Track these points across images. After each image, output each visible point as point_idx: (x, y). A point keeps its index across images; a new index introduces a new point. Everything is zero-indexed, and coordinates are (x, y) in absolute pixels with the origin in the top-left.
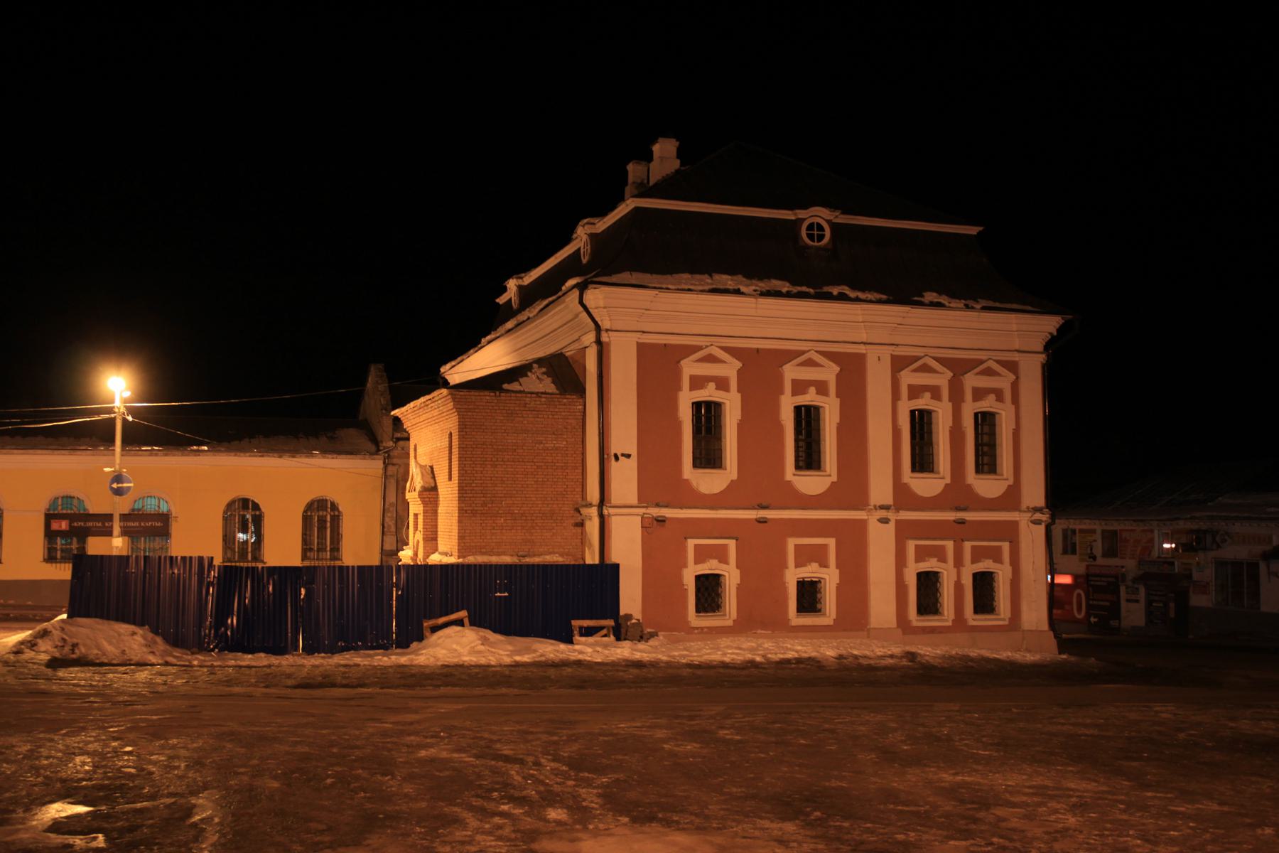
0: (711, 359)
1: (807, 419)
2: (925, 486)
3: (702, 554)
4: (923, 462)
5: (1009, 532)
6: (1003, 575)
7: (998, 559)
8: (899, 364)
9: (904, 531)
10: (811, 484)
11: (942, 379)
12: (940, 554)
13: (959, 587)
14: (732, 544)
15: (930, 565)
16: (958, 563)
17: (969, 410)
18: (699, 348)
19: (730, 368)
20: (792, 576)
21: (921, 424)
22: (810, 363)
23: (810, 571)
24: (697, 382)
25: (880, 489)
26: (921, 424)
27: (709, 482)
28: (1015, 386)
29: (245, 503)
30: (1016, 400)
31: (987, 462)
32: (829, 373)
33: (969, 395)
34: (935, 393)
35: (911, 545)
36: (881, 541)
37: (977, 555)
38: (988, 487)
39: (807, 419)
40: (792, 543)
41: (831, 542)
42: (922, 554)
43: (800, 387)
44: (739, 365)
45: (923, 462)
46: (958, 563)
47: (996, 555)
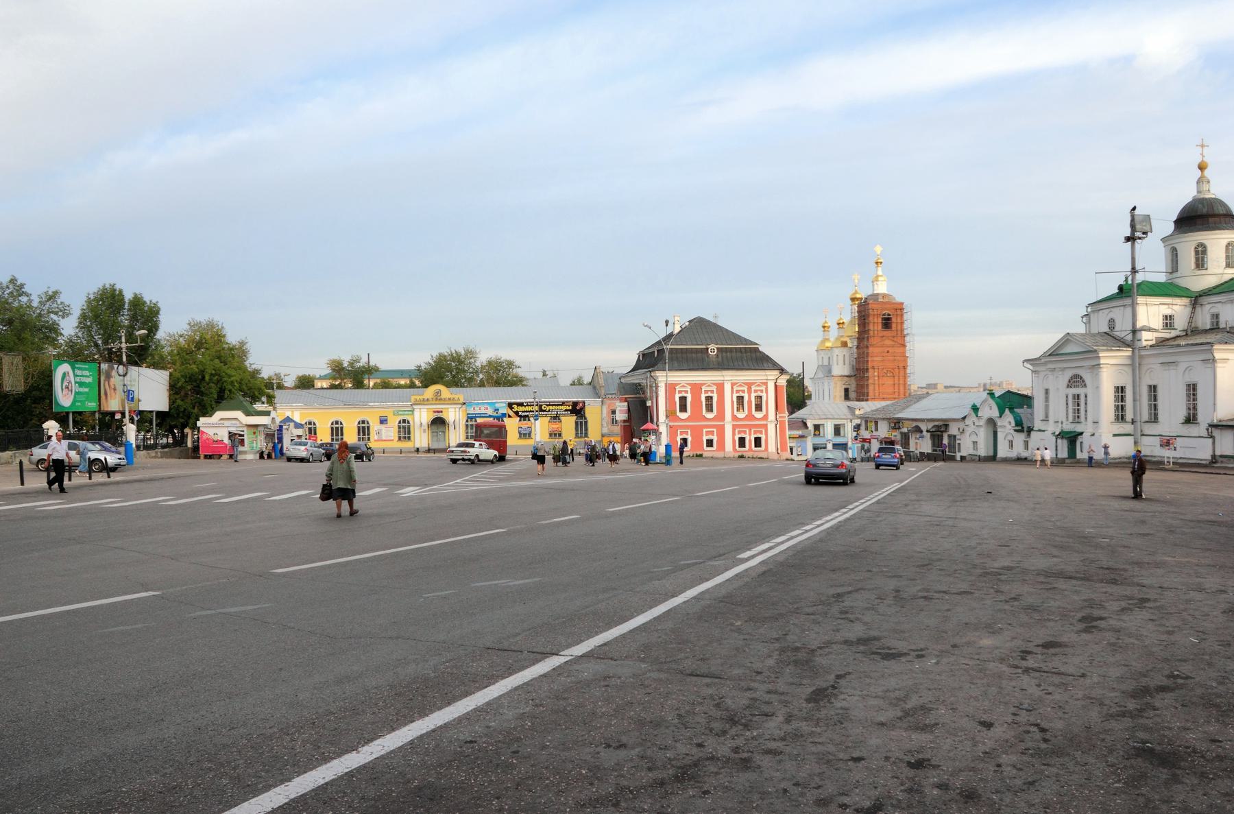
0: (683, 386)
1: (709, 399)
2: (741, 415)
3: (682, 433)
5: (765, 426)
7: (762, 433)
8: (733, 385)
9: (734, 427)
10: (710, 416)
11: (745, 388)
12: (745, 432)
13: (750, 441)
14: (689, 431)
16: (750, 434)
17: (753, 395)
18: (679, 384)
19: (688, 389)
20: (705, 438)
21: (740, 399)
22: (709, 386)
23: (710, 437)
24: (680, 392)
26: (740, 399)
27: (683, 416)
28: (766, 389)
30: (767, 393)
31: (759, 408)
32: (714, 388)
33: (703, 392)
34: (743, 391)
35: (737, 431)
38: (759, 415)
39: (709, 399)
40: (704, 430)
41: (715, 430)
42: (739, 432)
43: (706, 392)
44: (690, 387)
46: (750, 434)
47: (761, 433)
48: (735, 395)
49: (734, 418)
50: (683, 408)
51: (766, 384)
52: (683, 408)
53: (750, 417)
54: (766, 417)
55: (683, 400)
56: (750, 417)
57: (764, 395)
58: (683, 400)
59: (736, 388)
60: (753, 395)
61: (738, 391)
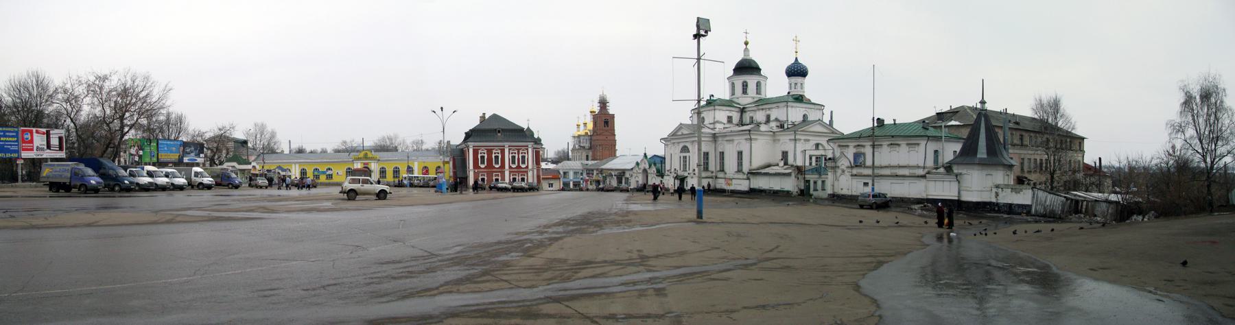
2: (514, 166)
3: (482, 175)
4: (513, 162)
5: (527, 172)
6: (526, 177)
8: (509, 150)
9: (510, 172)
11: (516, 152)
15: (514, 177)
20: (494, 178)
21: (513, 158)
25: (507, 166)
26: (513, 158)
29: (425, 167)
31: (523, 162)
36: (507, 173)
37: (521, 175)
38: (523, 166)
39: (497, 157)
45: (513, 162)
48: (511, 155)
49: (510, 167)
50: (483, 162)
51: (527, 149)
52: (483, 162)
53: (519, 167)
54: (527, 167)
55: (483, 157)
56: (519, 167)
57: (526, 155)
58: (483, 157)
59: (511, 152)
60: (520, 155)
61: (512, 153)
